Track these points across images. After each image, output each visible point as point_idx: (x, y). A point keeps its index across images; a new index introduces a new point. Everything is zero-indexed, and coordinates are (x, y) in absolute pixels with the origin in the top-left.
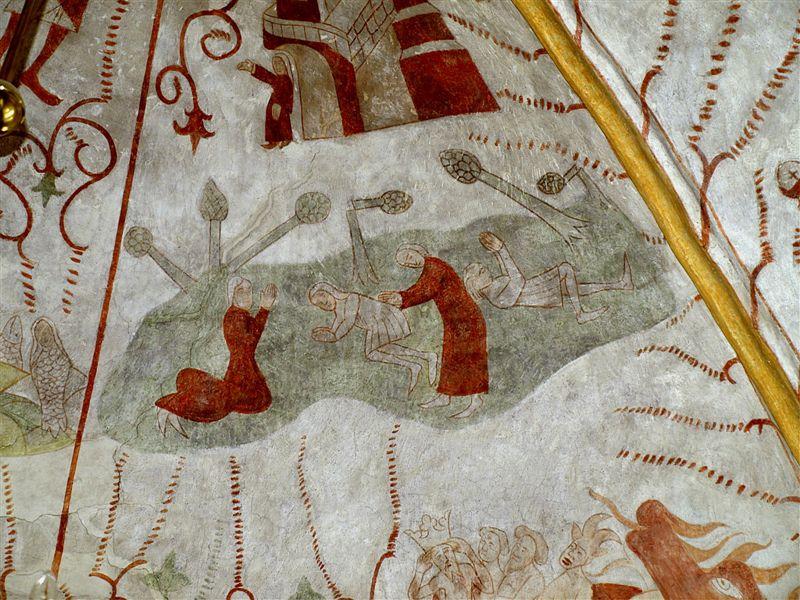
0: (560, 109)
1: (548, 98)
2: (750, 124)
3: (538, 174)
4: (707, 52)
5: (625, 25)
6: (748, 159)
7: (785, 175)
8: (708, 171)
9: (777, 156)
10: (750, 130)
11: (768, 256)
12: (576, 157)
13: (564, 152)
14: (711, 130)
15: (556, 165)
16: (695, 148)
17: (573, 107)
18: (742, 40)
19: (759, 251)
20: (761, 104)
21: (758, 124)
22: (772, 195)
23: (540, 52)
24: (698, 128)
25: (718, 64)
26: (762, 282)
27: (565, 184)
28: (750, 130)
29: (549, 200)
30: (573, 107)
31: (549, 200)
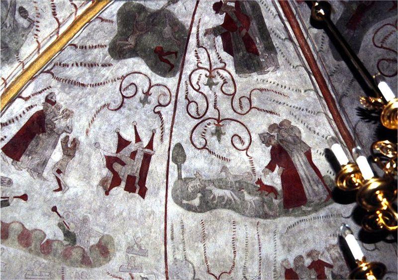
0: (54, 14)
1: (57, 9)
2: (63, 79)
3: (25, 7)
4: (82, 61)
5: (89, 34)
6: (54, 82)
7: (51, 96)
8: (48, 72)
9: (56, 91)
10: (62, 80)
11: (26, 99)
12: (38, 22)
13: (37, 17)
14: (61, 69)
15: (32, 13)
16: (54, 66)
17: (57, 20)
18: (85, 69)
19: (27, 96)
20: (69, 81)
21: (64, 82)
22: (45, 94)
23: (75, 6)
24: (60, 64)
25: (79, 64)
26: (18, 100)
27: (26, 18)
28: (62, 80)
29: (17, 13)
30: (57, 20)
31: (17, 13)
